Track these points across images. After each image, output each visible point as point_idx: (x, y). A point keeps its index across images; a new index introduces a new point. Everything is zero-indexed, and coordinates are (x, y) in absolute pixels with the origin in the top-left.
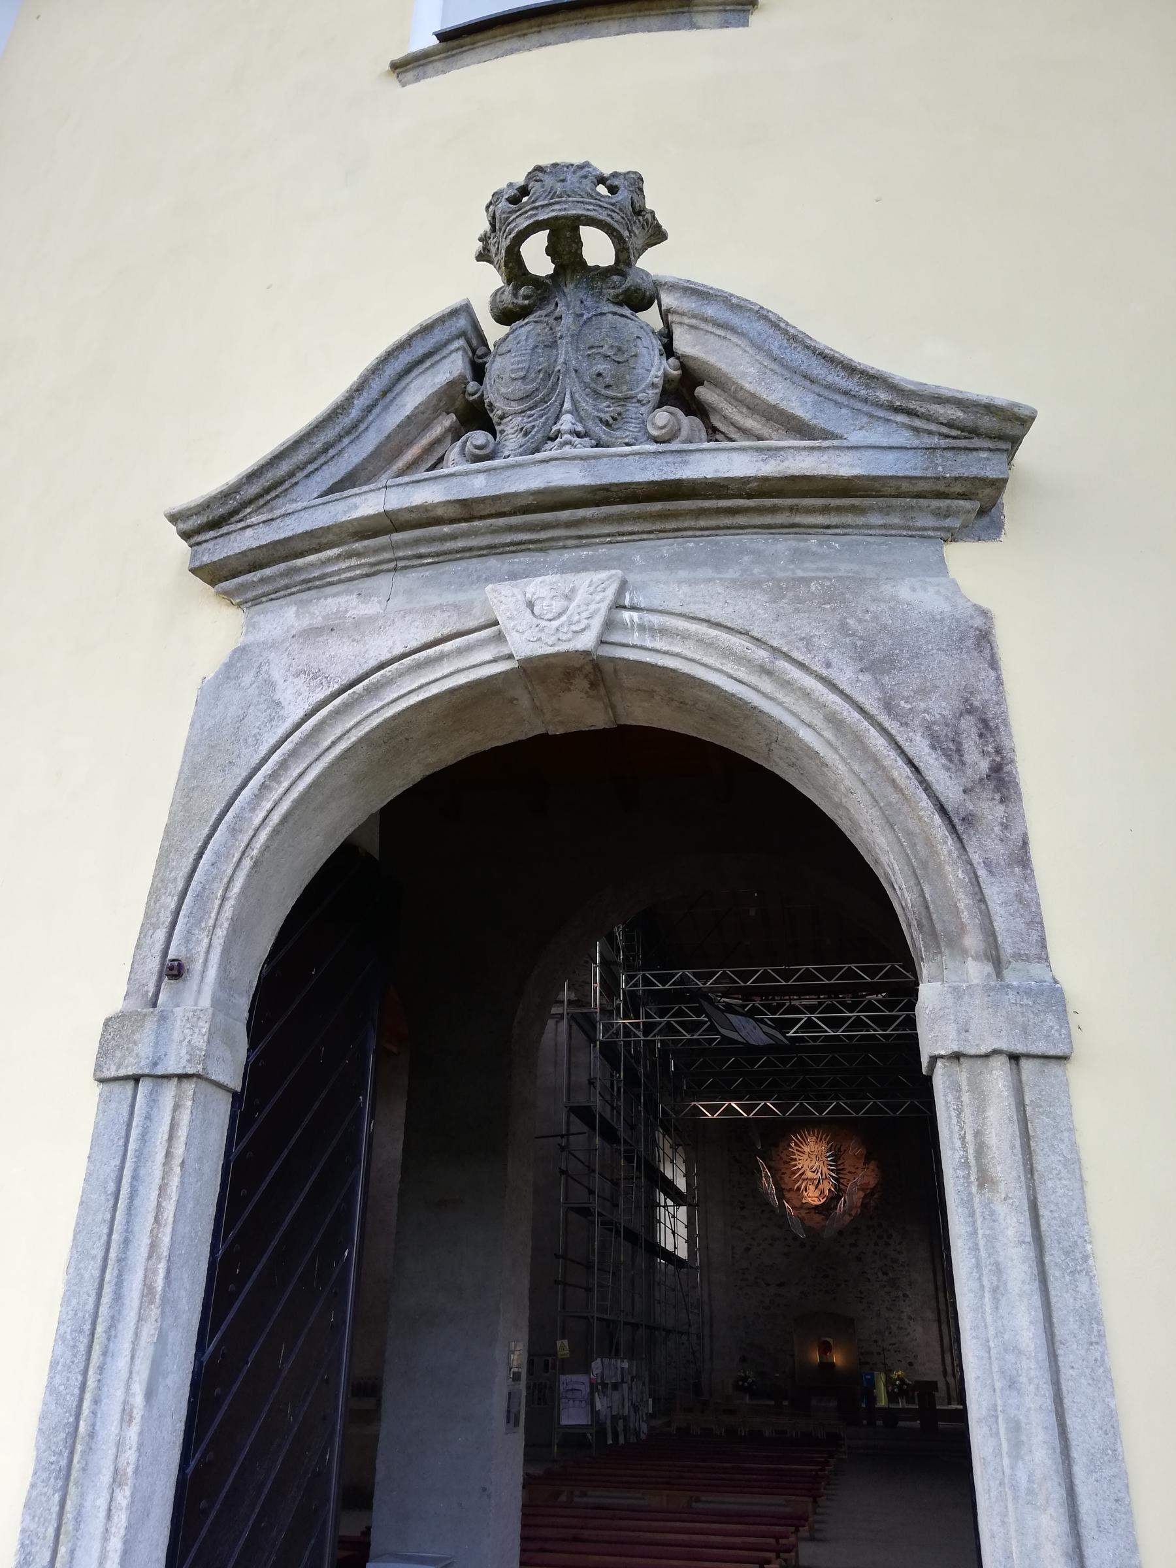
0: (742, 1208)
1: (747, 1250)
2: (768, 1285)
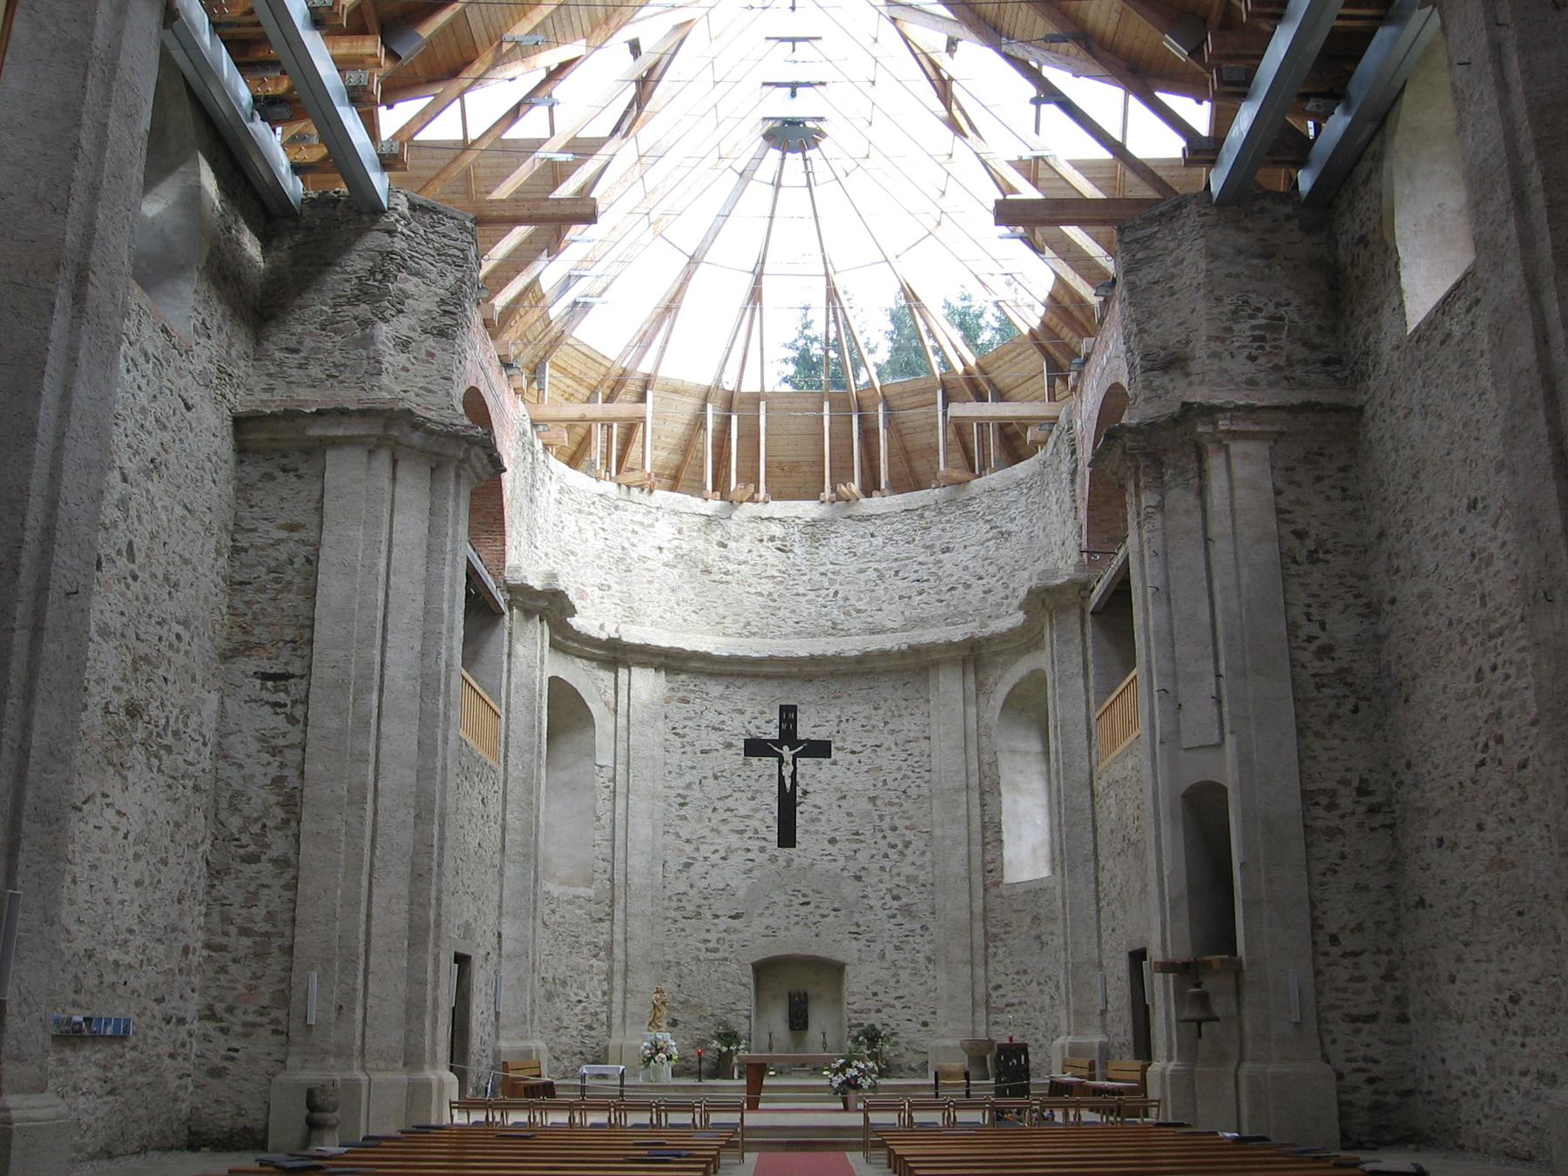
0: (682, 805)
1: (688, 865)
2: (717, 916)
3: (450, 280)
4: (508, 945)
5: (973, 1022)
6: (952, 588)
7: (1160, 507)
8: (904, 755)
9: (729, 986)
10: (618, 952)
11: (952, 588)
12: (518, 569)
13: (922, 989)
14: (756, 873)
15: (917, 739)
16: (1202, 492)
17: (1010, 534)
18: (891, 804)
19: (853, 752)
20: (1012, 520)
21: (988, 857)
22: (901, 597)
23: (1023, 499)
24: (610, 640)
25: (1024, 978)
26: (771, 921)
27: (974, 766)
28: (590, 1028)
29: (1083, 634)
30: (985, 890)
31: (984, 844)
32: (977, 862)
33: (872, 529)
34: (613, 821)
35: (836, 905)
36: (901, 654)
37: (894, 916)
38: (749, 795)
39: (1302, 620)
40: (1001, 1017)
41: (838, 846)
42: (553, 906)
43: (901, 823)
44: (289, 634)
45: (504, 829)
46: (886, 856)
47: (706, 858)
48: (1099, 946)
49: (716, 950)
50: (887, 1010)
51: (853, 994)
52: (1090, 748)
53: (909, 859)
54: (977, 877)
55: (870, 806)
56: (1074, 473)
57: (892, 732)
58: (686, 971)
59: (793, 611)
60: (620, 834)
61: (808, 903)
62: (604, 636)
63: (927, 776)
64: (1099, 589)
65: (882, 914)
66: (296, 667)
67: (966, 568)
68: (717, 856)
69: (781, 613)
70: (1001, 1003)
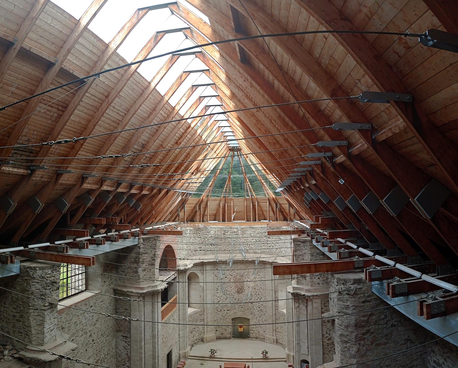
4: (181, 336)
7: (299, 307)
10: (205, 320)
16: (307, 307)
26: (235, 311)
27: (273, 286)
39: (325, 334)
44: (127, 330)
54: (274, 307)
60: (205, 298)
66: (128, 336)
70: (278, 331)
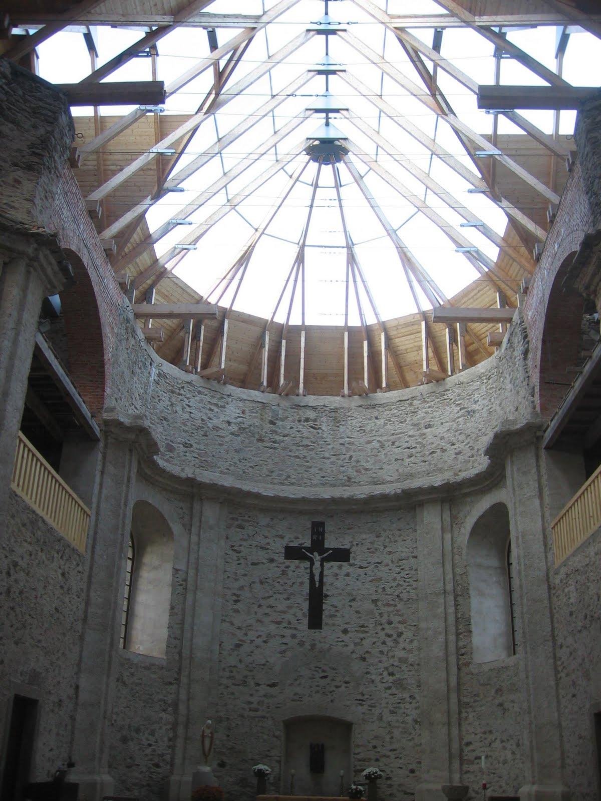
0: (236, 601)
1: (238, 646)
2: (258, 685)
3: (41, 131)
4: (83, 696)
5: (450, 771)
6: (433, 452)
8: (398, 570)
9: (265, 737)
10: (182, 708)
11: (433, 452)
12: (112, 410)
13: (411, 744)
14: (289, 654)
15: (407, 558)
17: (474, 412)
18: (388, 605)
19: (361, 567)
20: (476, 402)
21: (461, 644)
22: (396, 460)
23: (484, 387)
24: (188, 479)
25: (490, 737)
27: (450, 576)
28: (157, 766)
29: (538, 466)
30: (459, 669)
31: (458, 634)
32: (452, 647)
33: (376, 413)
34: (183, 610)
35: (347, 679)
36: (397, 497)
37: (389, 688)
38: (285, 596)
40: (472, 768)
41: (349, 635)
42: (132, 670)
43: (396, 619)
45: (87, 603)
46: (384, 643)
47: (252, 641)
48: (558, 710)
49: (256, 710)
50: (383, 760)
51: (358, 746)
52: (546, 552)
53: (401, 646)
54: (453, 659)
55: (372, 606)
56: (526, 353)
57: (390, 553)
58: (234, 725)
59: (321, 469)
60: (188, 619)
61: (326, 677)
62: (183, 475)
63: (415, 584)
64: (553, 425)
65: (381, 686)
67: (442, 438)
68: (260, 640)
69: (312, 470)
70: (471, 756)
